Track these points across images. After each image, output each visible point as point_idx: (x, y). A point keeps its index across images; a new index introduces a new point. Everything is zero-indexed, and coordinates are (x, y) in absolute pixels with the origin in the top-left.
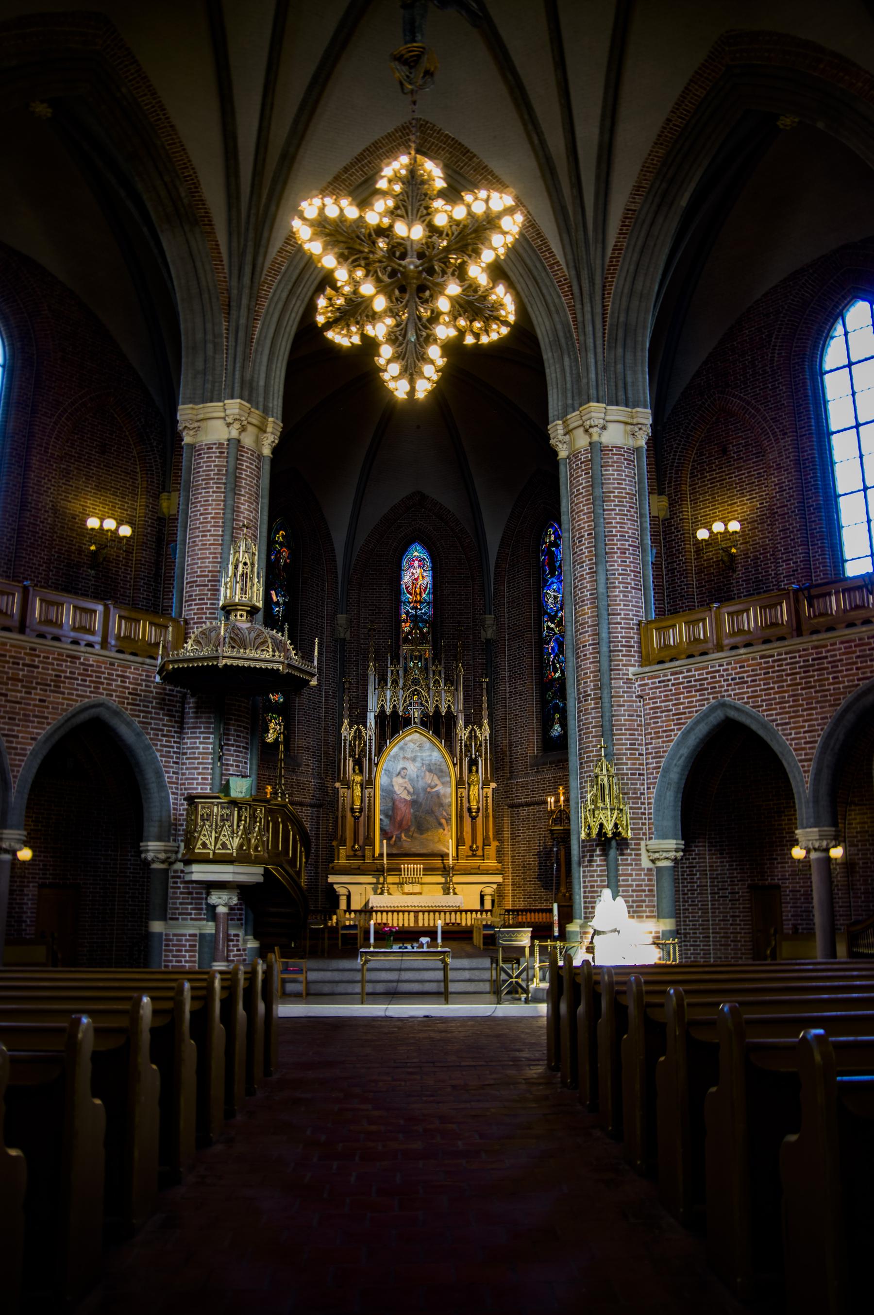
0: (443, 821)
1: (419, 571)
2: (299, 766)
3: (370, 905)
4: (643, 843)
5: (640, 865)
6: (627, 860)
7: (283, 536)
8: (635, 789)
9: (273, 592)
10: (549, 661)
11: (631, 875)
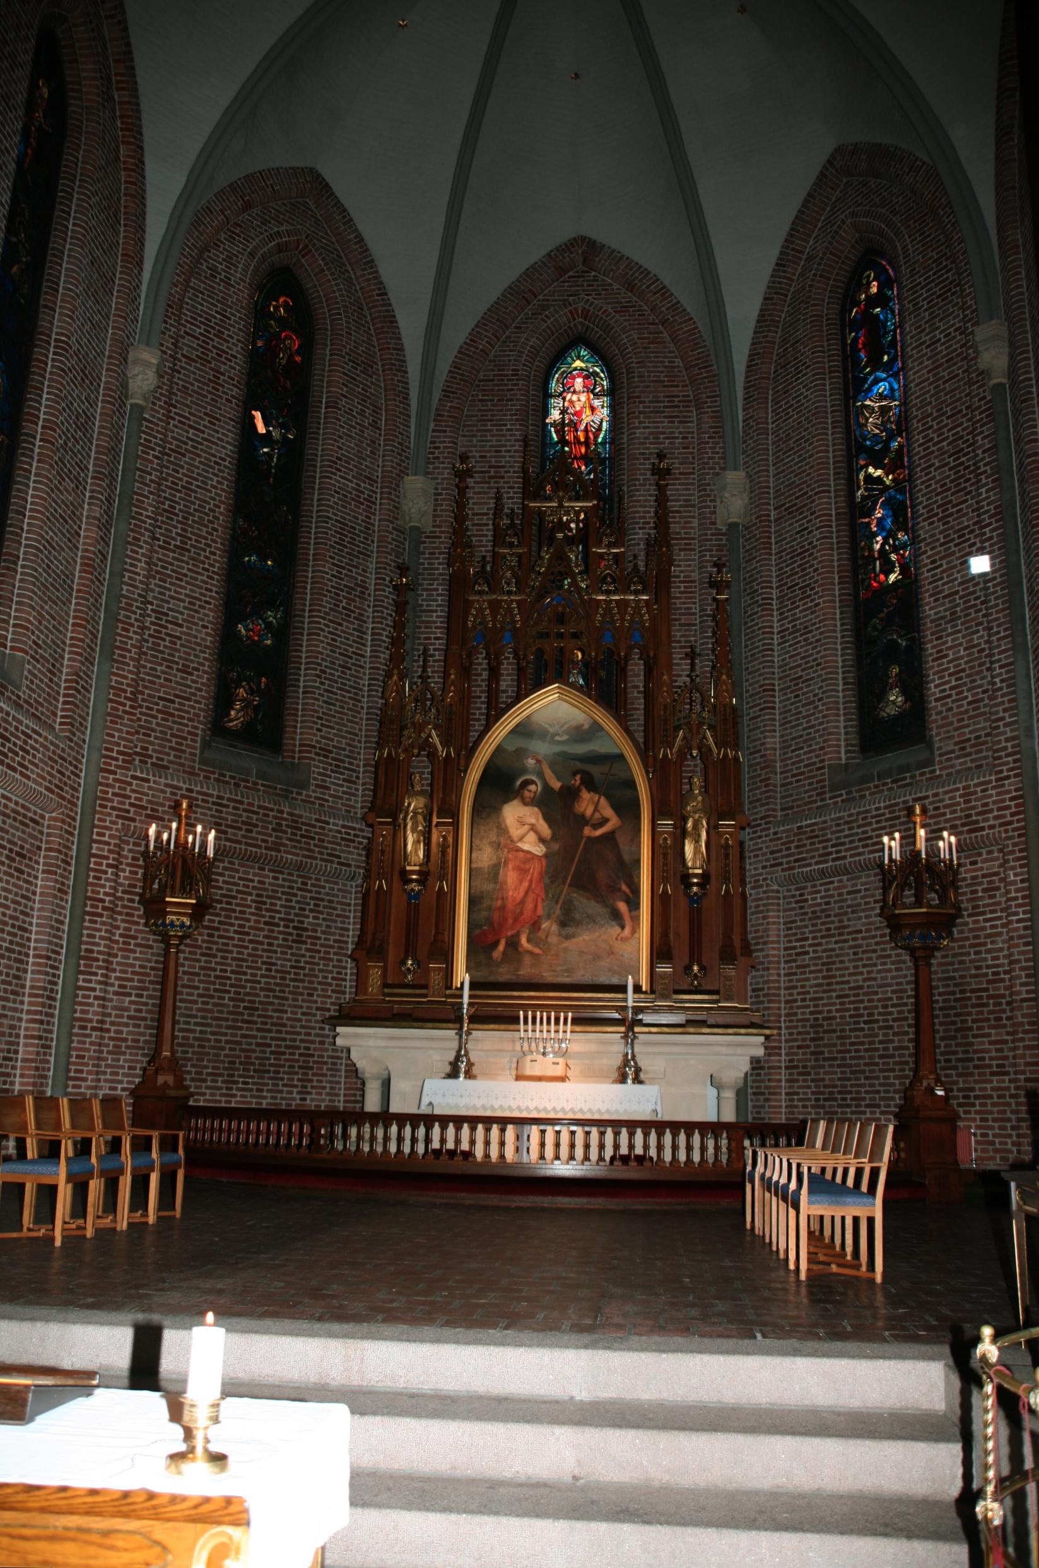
0: (622, 907)
1: (583, 397)
2: (304, 785)
3: (425, 1100)
7: (286, 303)
9: (258, 415)
10: (871, 549)
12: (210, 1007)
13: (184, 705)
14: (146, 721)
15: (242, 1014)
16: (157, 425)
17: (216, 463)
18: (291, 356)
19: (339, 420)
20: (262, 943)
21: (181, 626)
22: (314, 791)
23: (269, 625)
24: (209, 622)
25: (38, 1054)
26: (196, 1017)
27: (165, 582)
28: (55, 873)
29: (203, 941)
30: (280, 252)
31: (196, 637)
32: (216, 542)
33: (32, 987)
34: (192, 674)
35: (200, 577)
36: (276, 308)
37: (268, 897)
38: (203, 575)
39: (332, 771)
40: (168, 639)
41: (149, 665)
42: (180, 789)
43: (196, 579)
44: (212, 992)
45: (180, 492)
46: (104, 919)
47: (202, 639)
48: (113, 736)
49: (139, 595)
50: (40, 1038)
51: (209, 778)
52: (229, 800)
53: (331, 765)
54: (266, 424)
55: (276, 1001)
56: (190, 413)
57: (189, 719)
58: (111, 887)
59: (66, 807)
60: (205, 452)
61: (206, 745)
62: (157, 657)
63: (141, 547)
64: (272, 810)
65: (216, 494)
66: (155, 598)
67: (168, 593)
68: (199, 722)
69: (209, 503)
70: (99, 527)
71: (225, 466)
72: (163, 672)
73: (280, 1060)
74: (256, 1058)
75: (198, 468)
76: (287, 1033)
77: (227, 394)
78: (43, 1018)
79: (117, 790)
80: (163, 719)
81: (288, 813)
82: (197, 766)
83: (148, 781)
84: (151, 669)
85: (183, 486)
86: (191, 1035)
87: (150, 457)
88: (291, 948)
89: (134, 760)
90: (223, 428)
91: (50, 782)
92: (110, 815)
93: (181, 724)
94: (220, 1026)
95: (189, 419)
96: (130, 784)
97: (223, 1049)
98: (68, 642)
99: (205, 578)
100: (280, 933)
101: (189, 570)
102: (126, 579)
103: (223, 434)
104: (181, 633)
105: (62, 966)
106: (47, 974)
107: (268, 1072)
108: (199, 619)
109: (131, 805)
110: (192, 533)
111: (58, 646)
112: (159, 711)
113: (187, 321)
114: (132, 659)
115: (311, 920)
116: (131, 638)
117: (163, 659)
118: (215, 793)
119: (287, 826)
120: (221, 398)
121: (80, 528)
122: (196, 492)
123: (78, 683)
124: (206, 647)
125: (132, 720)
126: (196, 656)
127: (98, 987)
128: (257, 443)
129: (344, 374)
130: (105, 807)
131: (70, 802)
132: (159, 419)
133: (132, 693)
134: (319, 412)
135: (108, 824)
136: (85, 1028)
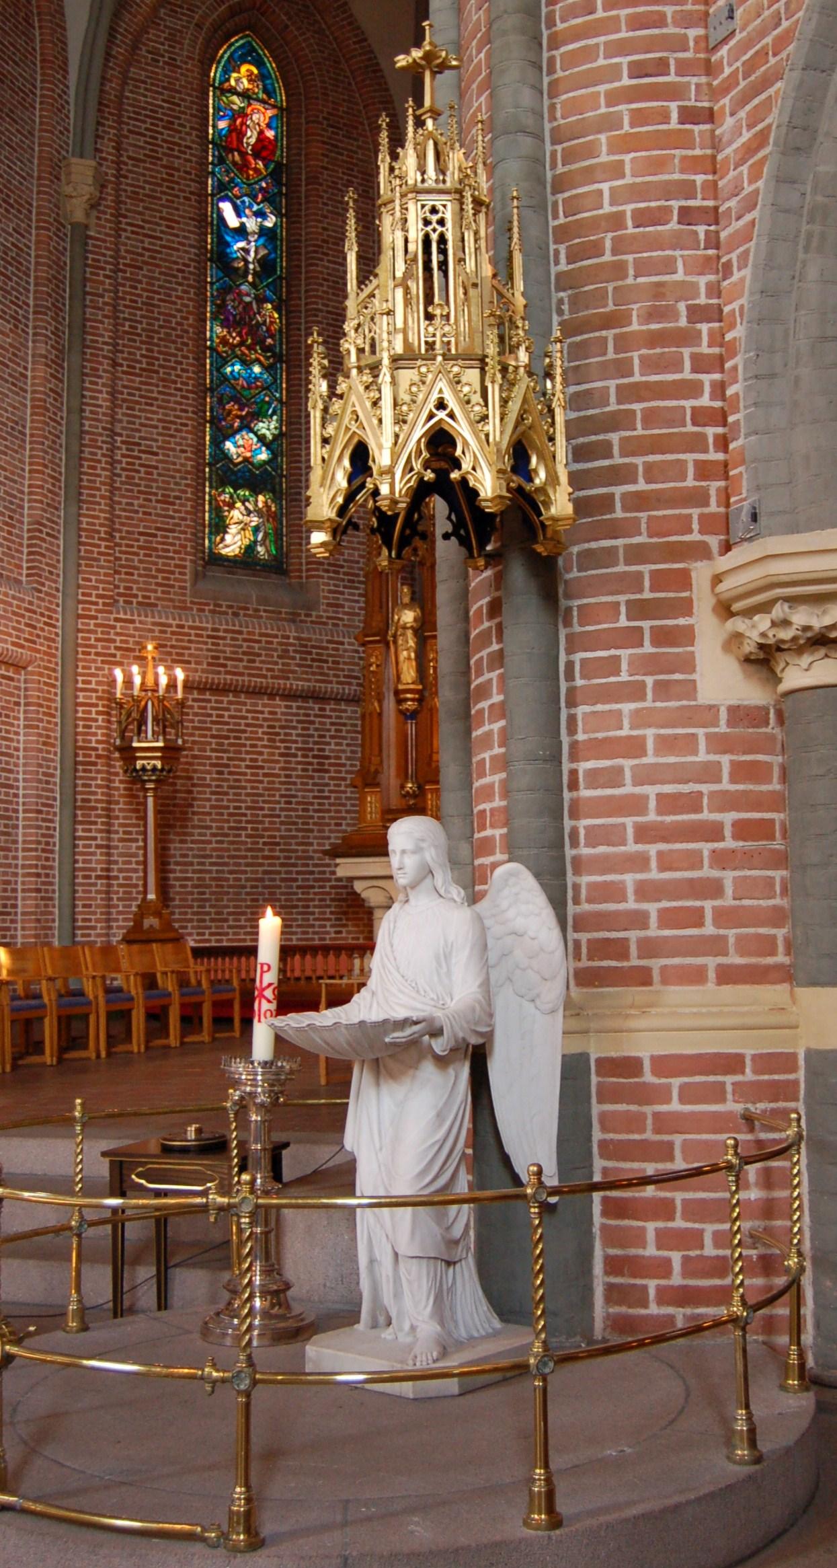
4: (701, 572)
5: (690, 689)
6: (613, 666)
8: (658, 291)
11: (635, 747)
12: (225, 846)
13: (167, 537)
14: (127, 560)
15: (262, 850)
16: (104, 241)
17: (179, 270)
18: (261, 133)
19: (322, 197)
20: (278, 776)
21: (156, 454)
22: (325, 611)
23: (261, 439)
24: (187, 445)
25: (37, 906)
26: (211, 857)
27: (133, 409)
28: (37, 727)
29: (212, 779)
30: (232, 16)
31: (174, 464)
32: (188, 358)
33: (24, 842)
34: (173, 504)
35: (172, 399)
36: (238, 80)
37: (282, 727)
38: (176, 396)
39: (345, 587)
40: (142, 469)
41: (124, 501)
42: (170, 626)
43: (169, 402)
44: (226, 831)
45: (141, 309)
46: (99, 767)
47: (182, 465)
48: (90, 580)
49: (104, 428)
50: (38, 891)
51: (203, 611)
52: (226, 631)
53: (343, 580)
54: (239, 213)
55: (300, 834)
56: (143, 221)
57: (175, 552)
58: (103, 735)
59: (42, 660)
60: (165, 260)
61: (197, 576)
62: (131, 491)
63: (100, 377)
64: (276, 636)
65: (183, 305)
66: (123, 428)
67: (137, 421)
68: (186, 553)
69: (175, 317)
70: (47, 365)
71: (190, 273)
72: (141, 506)
73: (308, 893)
74: (282, 894)
75: (159, 280)
76: (316, 865)
77: (184, 191)
78: (40, 871)
79: (100, 636)
80: (145, 555)
81: (295, 638)
82: (188, 599)
83: (132, 622)
84: (127, 504)
85: (143, 303)
86: (208, 876)
87: (101, 278)
88: (312, 777)
89: (117, 601)
90: (184, 231)
91: (18, 637)
92: (94, 661)
93: (167, 558)
94: (239, 865)
95: (143, 228)
96: (114, 627)
97: (244, 887)
98: (26, 490)
99: (178, 399)
100: (299, 763)
101: (159, 392)
102: (87, 414)
103: (185, 237)
104: (157, 461)
105: (58, 818)
106: (39, 827)
107: (296, 907)
108: (176, 444)
109: (117, 648)
110: (159, 352)
111: (15, 497)
112: (140, 547)
113: (130, 118)
114: (102, 497)
115: (333, 747)
116: (99, 476)
117: (139, 492)
118: (210, 626)
119: (295, 651)
120: (177, 196)
121: (26, 368)
122: (159, 307)
123: (41, 531)
124: (187, 472)
125: (109, 561)
126: (176, 484)
127: (99, 835)
128: (228, 239)
129: (324, 143)
130: (89, 654)
131: (45, 653)
132: (107, 235)
133: (106, 533)
134: (300, 192)
135: (93, 671)
136: (89, 877)
